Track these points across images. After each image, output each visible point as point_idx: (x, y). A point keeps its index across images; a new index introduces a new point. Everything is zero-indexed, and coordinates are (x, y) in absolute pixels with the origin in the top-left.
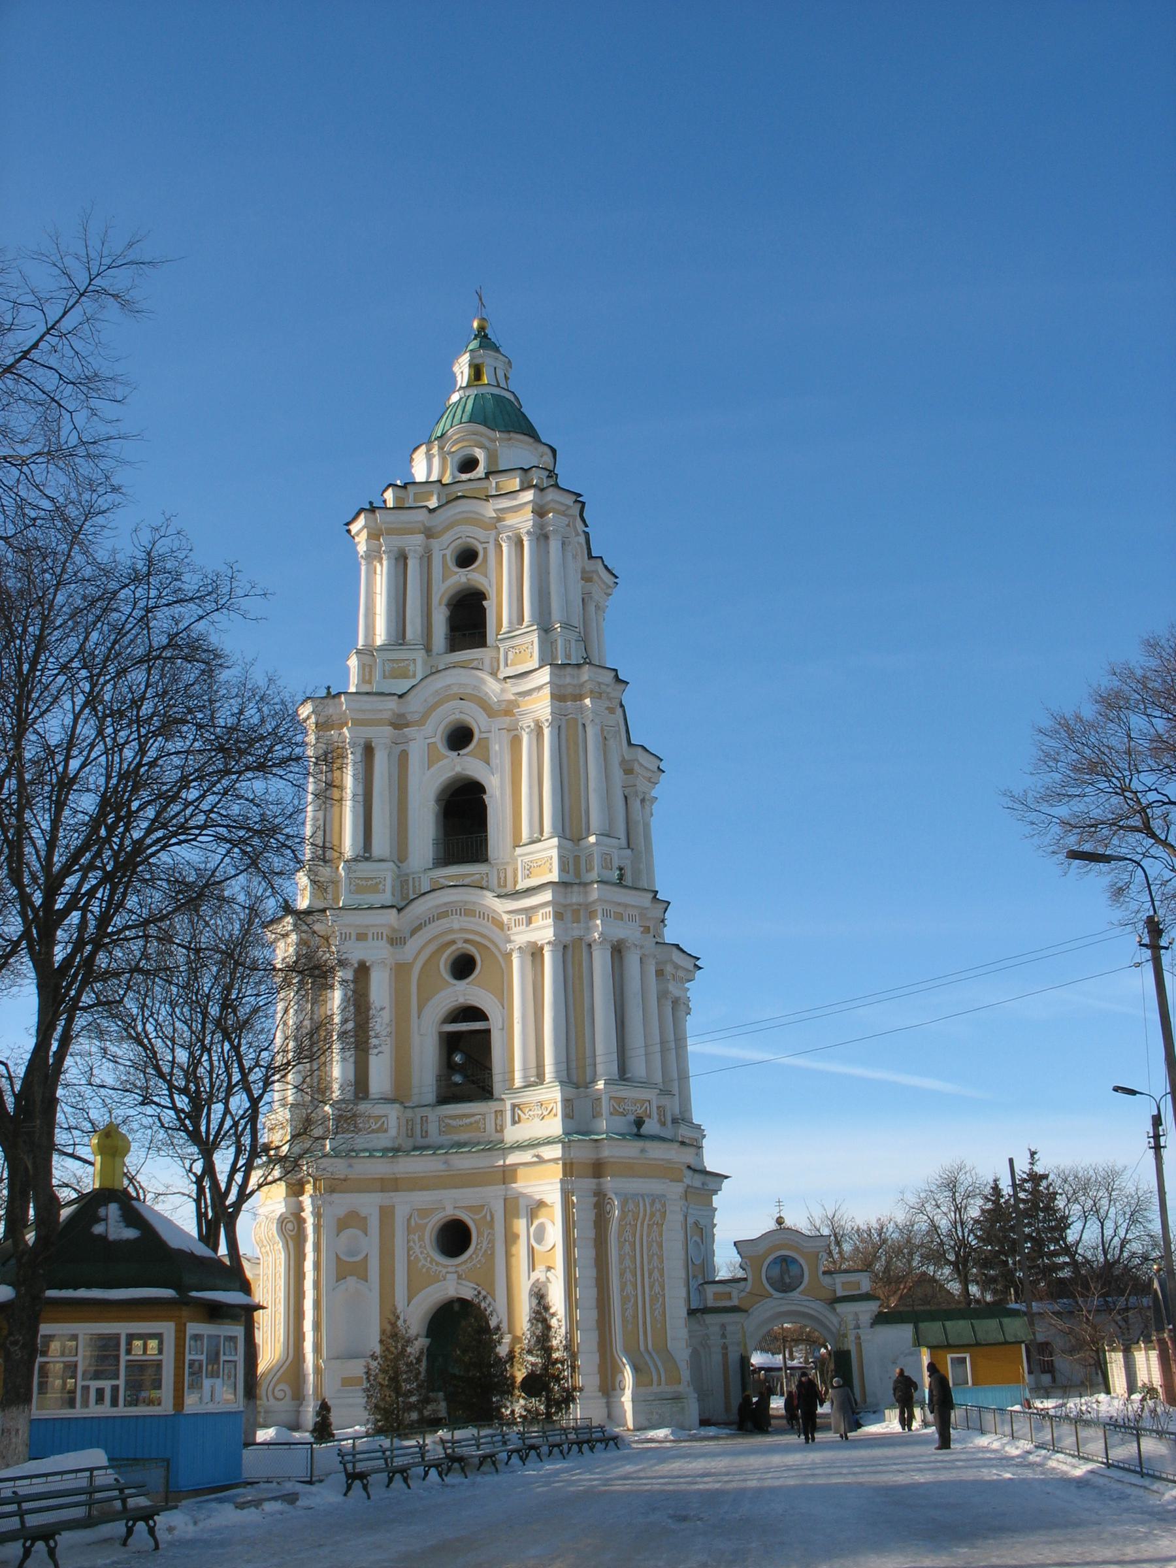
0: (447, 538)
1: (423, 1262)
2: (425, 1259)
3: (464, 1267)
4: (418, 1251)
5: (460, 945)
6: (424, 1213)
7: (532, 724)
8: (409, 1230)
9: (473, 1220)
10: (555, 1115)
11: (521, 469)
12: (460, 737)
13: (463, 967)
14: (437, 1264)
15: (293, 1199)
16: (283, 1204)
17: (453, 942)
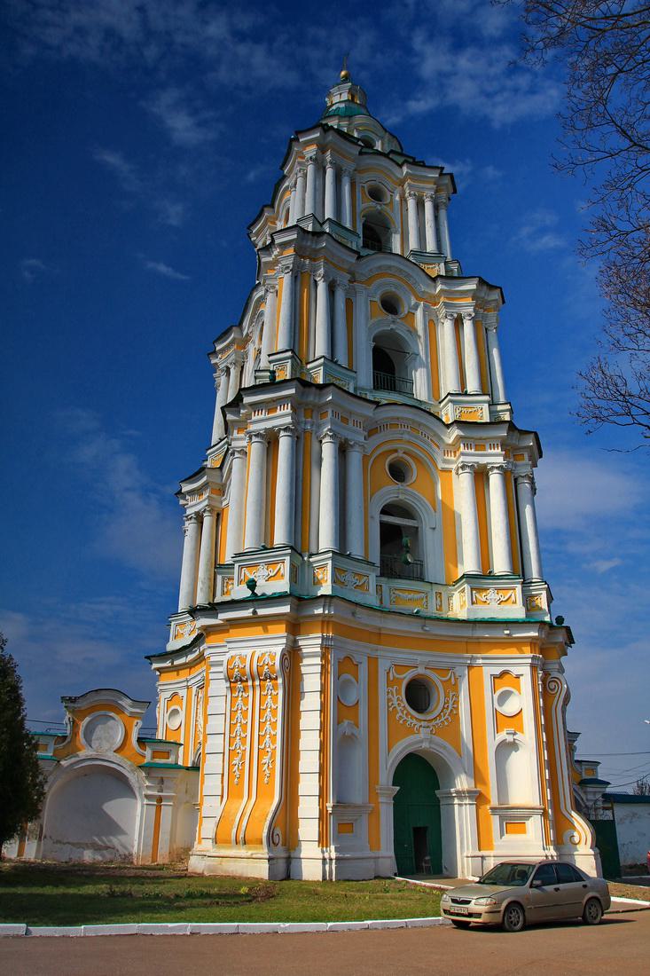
0: (367, 176)
1: (400, 714)
2: (402, 712)
3: (433, 723)
4: (396, 703)
5: (400, 454)
6: (400, 668)
7: (455, 315)
8: (389, 684)
9: (442, 682)
10: (515, 602)
11: (414, 159)
12: (390, 305)
13: (398, 472)
14: (412, 717)
15: (291, 637)
16: (284, 641)
17: (396, 451)
